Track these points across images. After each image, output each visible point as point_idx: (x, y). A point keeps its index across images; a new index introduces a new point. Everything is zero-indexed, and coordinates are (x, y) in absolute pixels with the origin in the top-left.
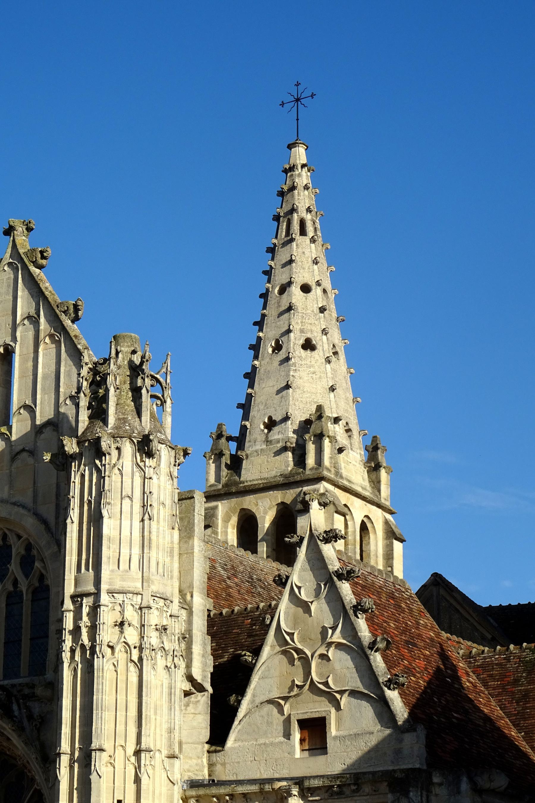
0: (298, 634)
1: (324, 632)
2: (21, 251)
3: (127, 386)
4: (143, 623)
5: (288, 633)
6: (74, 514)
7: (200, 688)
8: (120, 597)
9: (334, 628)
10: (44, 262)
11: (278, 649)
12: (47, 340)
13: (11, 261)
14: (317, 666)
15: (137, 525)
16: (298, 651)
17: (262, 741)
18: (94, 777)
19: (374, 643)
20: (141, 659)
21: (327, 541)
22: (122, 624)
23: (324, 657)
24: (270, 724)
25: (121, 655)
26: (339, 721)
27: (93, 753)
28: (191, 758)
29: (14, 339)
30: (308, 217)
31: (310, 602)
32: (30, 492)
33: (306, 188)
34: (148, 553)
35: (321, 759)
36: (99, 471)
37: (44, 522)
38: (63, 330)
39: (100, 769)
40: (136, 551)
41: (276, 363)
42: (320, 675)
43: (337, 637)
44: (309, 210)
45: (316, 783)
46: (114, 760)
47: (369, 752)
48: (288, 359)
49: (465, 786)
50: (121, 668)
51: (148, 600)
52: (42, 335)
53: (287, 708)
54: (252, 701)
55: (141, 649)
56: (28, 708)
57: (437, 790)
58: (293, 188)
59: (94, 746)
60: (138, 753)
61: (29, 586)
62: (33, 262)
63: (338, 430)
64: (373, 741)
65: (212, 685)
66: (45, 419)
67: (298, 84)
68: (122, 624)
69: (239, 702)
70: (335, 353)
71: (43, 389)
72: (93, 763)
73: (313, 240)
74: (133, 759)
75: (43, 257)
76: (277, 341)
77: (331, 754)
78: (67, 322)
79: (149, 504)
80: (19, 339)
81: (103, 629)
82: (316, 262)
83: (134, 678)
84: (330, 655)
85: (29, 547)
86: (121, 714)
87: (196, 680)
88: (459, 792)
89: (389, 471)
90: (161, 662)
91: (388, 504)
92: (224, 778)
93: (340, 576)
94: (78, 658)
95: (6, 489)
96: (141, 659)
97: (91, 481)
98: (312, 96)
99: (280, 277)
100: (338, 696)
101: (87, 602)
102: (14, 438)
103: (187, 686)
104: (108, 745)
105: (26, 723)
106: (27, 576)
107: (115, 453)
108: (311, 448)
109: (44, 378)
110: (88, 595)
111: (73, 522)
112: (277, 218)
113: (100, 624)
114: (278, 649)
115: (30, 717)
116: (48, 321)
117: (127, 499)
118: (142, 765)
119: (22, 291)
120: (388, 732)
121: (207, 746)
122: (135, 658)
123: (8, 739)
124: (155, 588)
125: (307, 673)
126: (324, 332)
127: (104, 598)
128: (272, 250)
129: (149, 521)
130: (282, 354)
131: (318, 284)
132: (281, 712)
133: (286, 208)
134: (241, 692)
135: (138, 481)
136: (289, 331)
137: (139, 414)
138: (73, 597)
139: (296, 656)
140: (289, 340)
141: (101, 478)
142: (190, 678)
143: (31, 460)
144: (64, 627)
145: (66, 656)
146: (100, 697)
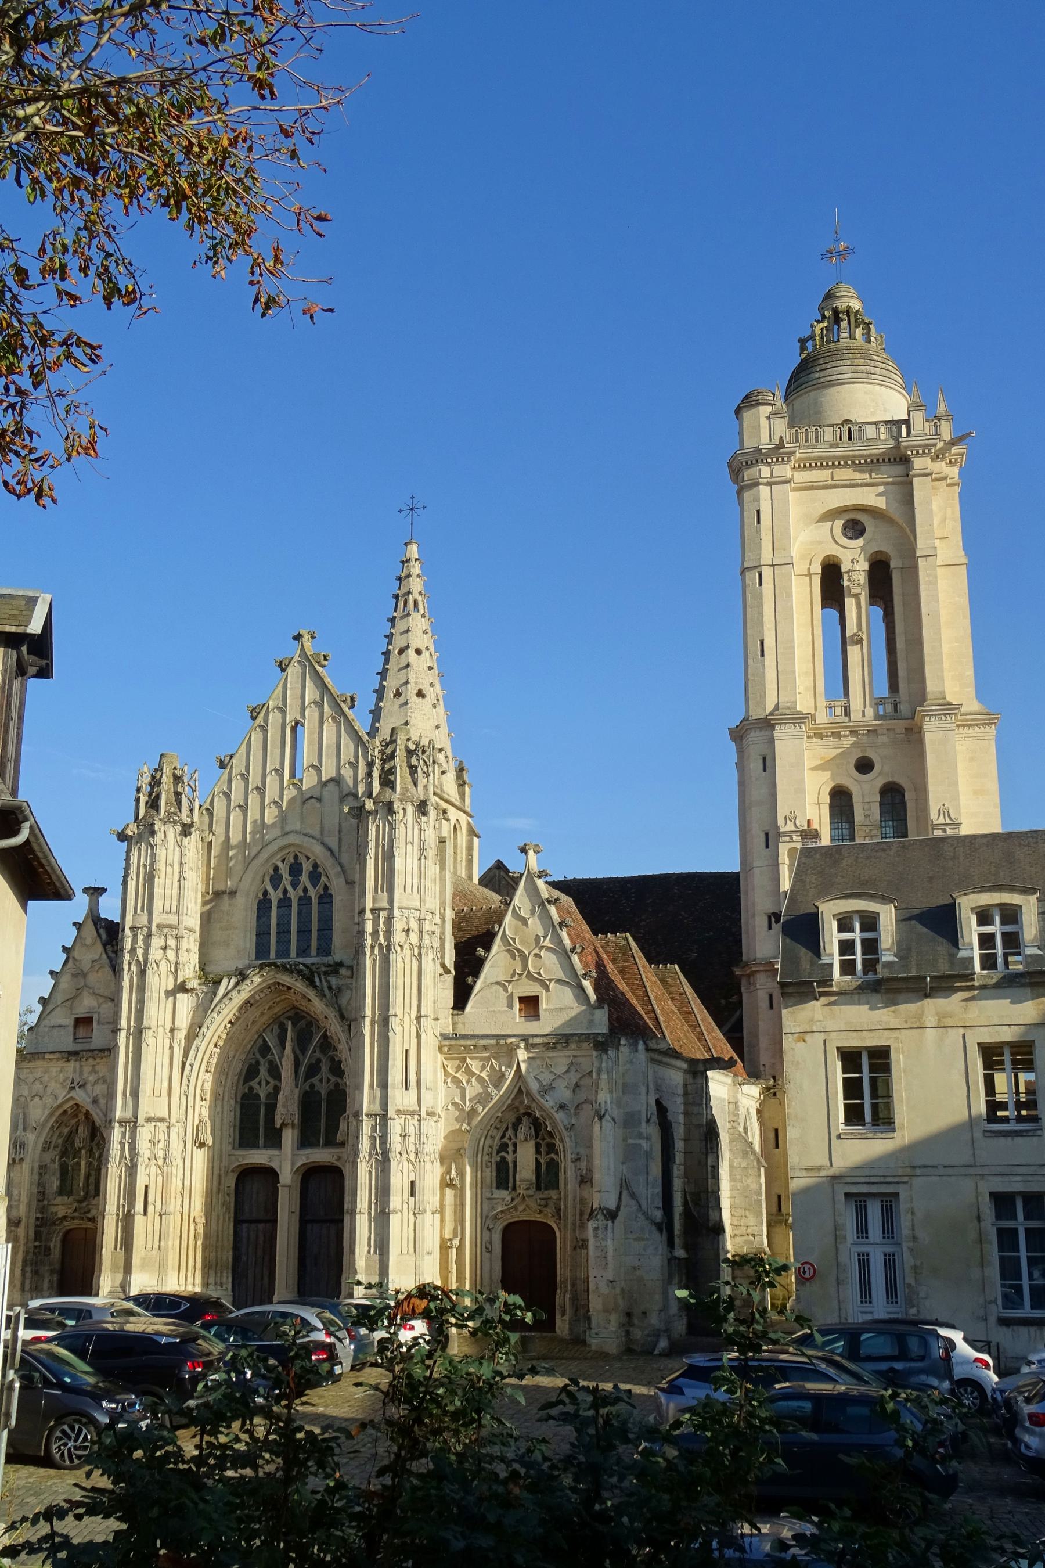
1: (537, 938)
2: (308, 654)
3: (405, 764)
6: (372, 852)
7: (447, 971)
8: (406, 912)
9: (545, 937)
10: (326, 663)
12: (330, 720)
15: (416, 862)
16: (518, 950)
17: (492, 1009)
19: (574, 948)
20: (420, 954)
21: (540, 877)
22: (408, 930)
24: (497, 998)
25: (407, 951)
29: (303, 716)
30: (420, 598)
32: (318, 828)
33: (418, 576)
35: (535, 1023)
36: (390, 823)
37: (330, 850)
38: (343, 713)
40: (416, 881)
41: (397, 706)
42: (534, 967)
43: (547, 943)
44: (420, 593)
45: (537, 1040)
47: (570, 1020)
48: (406, 703)
49: (641, 1046)
50: (407, 960)
52: (325, 717)
53: (510, 989)
54: (484, 982)
55: (420, 948)
56: (328, 981)
57: (622, 1049)
58: (409, 576)
59: (390, 1013)
60: (419, 1018)
61: (317, 892)
63: (440, 757)
64: (573, 1013)
65: (455, 969)
66: (328, 777)
67: (412, 498)
68: (408, 930)
69: (475, 982)
71: (327, 755)
73: (423, 616)
74: (415, 1022)
75: (325, 659)
76: (398, 690)
78: (346, 709)
82: (425, 632)
83: (415, 968)
85: (316, 866)
86: (407, 991)
88: (637, 1051)
89: (470, 787)
90: (431, 956)
91: (468, 809)
92: (464, 1033)
93: (550, 902)
94: (376, 951)
95: (299, 824)
96: (420, 954)
97: (384, 830)
98: (424, 507)
99: (399, 642)
101: (383, 915)
102: (304, 788)
103: (441, 970)
104: (399, 1013)
105: (326, 991)
106: (314, 886)
107: (401, 812)
109: (328, 746)
112: (396, 597)
114: (503, 948)
115: (330, 988)
116: (330, 706)
119: (309, 684)
120: (583, 1008)
122: (416, 953)
123: (309, 1000)
124: (427, 906)
125: (525, 965)
126: (432, 685)
127: (396, 913)
128: (392, 620)
130: (402, 700)
131: (427, 649)
132: (506, 990)
133: (404, 590)
134: (476, 974)
135: (417, 832)
136: (407, 683)
137: (415, 784)
138: (372, 910)
140: (407, 689)
141: (392, 829)
142: (443, 965)
143: (318, 805)
145: (368, 950)
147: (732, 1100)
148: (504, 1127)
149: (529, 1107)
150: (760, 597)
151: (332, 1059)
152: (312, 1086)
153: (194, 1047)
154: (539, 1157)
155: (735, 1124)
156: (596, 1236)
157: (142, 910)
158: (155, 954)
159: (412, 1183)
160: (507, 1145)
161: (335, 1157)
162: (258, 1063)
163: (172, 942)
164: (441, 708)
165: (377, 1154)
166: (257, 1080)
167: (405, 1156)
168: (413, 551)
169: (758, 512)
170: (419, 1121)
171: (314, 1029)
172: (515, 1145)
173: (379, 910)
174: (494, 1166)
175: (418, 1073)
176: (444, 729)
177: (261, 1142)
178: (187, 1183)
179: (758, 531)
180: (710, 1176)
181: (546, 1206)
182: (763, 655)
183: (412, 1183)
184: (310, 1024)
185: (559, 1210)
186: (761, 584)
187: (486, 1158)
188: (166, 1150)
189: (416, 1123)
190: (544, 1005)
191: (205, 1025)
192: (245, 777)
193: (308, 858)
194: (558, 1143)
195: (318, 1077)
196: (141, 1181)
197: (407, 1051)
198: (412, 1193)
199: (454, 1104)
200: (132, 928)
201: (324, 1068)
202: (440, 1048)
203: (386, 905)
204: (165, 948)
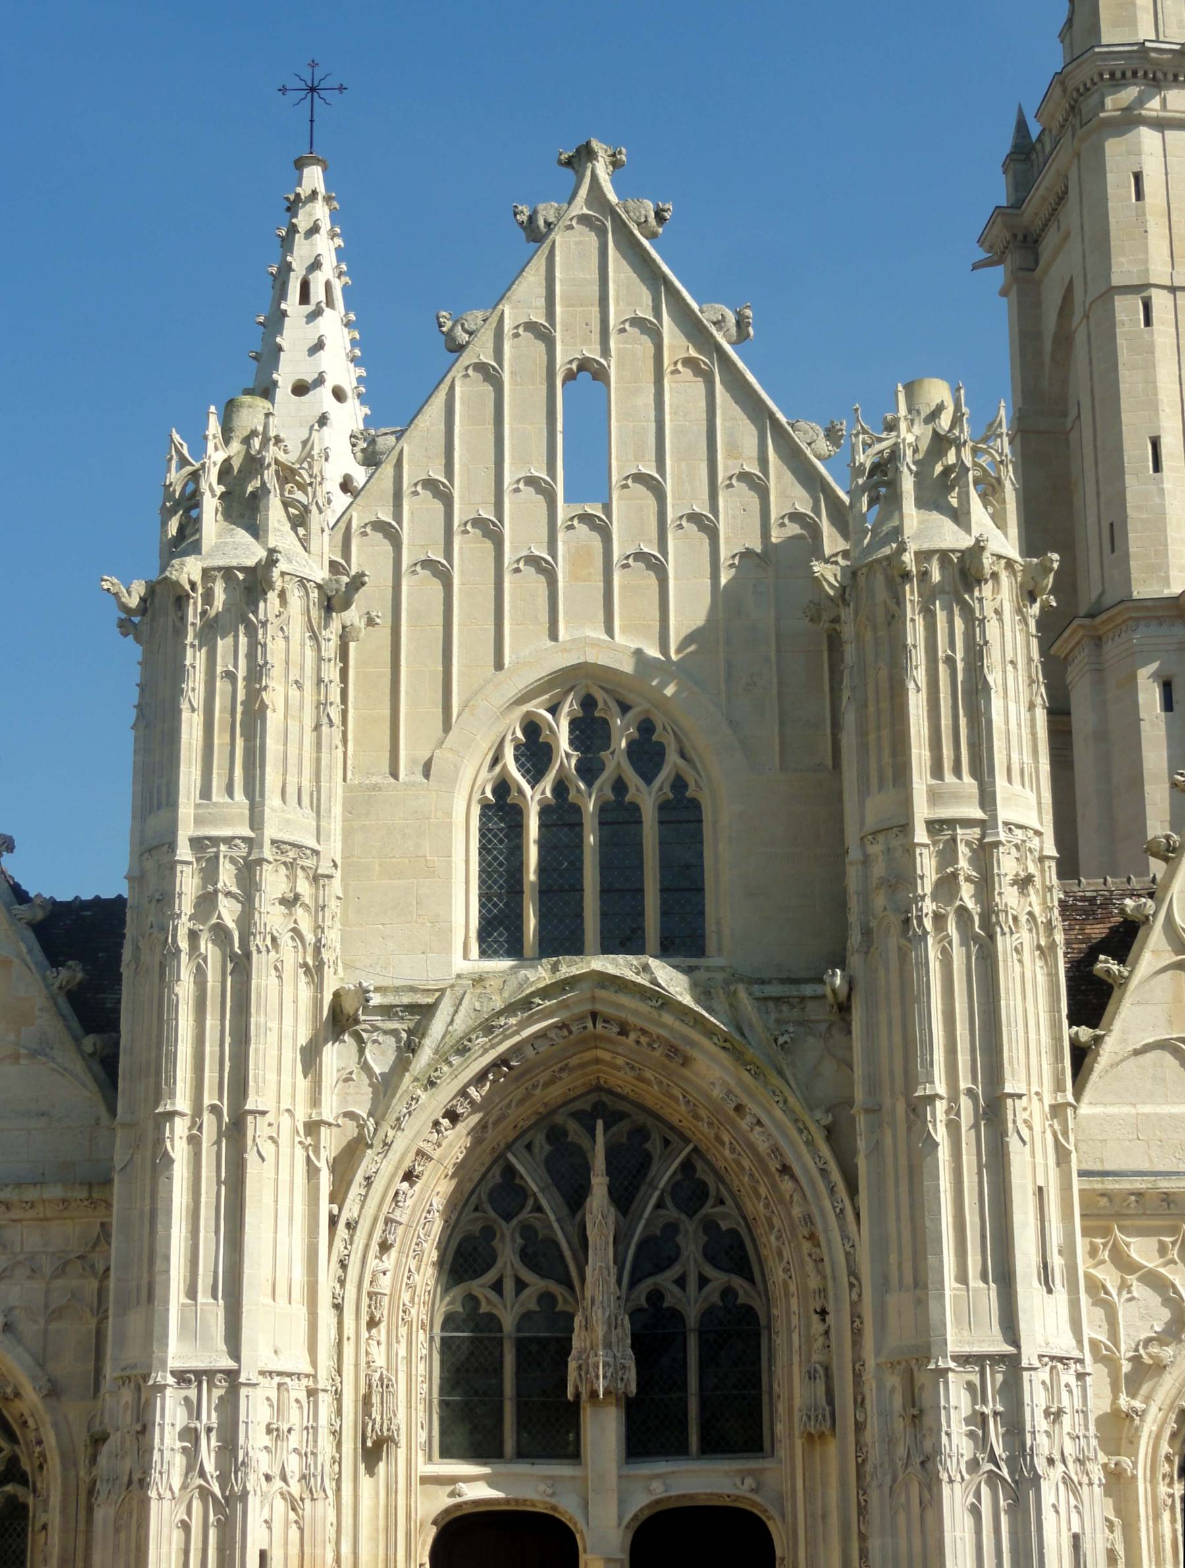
10: (660, 230)
13: (585, 211)
27: (1009, 1101)
62: (639, 224)
67: (313, 65)
69: (1098, 1040)
72: (1010, 1117)
80: (613, 353)
85: (646, 727)
109: (679, 432)
110: (967, 823)
144: (919, 872)
146: (1012, 1003)
150: (1151, 349)
151: (710, 1226)
152: (656, 1296)
153: (359, 1177)
157: (230, 791)
158: (271, 917)
159: (1076, 1538)
161: (749, 1482)
162: (489, 1232)
163: (304, 887)
165: (993, 1459)
166: (491, 1276)
167: (1060, 1467)
168: (314, 177)
169: (1138, 177)
170: (1081, 1376)
171: (654, 1146)
173: (951, 823)
177: (509, 1445)
178: (346, 1549)
179: (1141, 214)
182: (1157, 467)
184: (640, 1133)
186: (1148, 322)
188: (308, 1455)
189: (1072, 1380)
191: (391, 1118)
192: (441, 492)
193: (625, 708)
195: (675, 1271)
196: (256, 1538)
200: (197, 843)
201: (691, 1246)
203: (978, 814)
204: (290, 902)
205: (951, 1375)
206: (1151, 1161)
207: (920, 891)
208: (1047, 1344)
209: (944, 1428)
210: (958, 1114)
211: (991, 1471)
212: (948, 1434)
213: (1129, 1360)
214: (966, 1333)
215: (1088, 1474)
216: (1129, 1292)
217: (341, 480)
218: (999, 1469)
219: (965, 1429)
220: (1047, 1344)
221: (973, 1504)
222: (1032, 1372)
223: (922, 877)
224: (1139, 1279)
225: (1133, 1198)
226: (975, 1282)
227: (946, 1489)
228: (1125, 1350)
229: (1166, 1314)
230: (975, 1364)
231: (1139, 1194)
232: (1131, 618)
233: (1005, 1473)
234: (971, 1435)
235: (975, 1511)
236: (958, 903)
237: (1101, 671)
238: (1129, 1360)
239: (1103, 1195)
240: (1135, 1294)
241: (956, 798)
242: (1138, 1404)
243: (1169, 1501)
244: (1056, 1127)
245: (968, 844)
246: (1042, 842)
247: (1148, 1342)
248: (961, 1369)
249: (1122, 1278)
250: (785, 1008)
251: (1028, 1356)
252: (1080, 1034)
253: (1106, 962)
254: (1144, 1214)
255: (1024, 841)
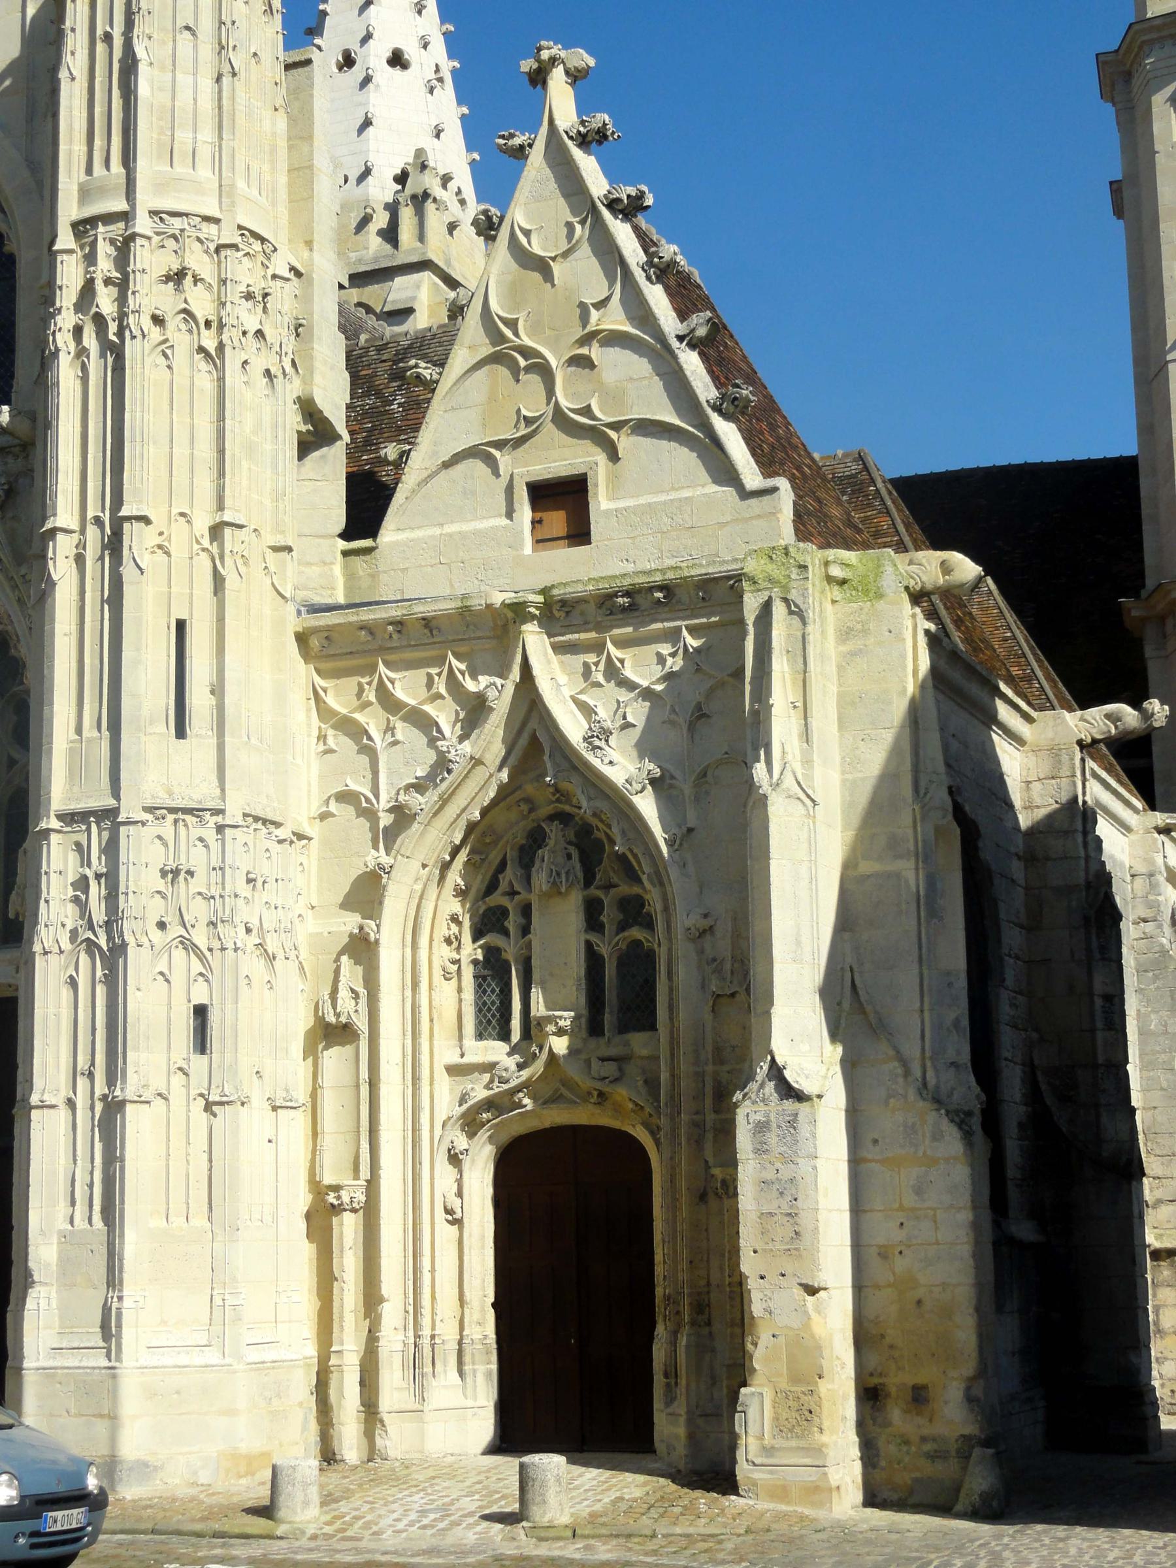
0: (526, 321)
4: (223, 276)
5: (506, 322)
11: (487, 350)
14: (566, 381)
15: (206, 83)
16: (526, 352)
18: (128, 571)
20: (221, 347)
23: (582, 362)
26: (615, 482)
27: (126, 526)
28: (309, 564)
31: (551, 258)
34: (230, 140)
39: (141, 556)
40: (206, 134)
46: (170, 541)
48: (367, 80)
51: (229, 235)
60: (216, 532)
63: (446, 196)
69: (404, 456)
70: (440, 80)
77: (599, 544)
79: (231, 45)
81: (142, 281)
84: (593, 356)
86: (181, 451)
87: (321, 412)
96: (221, 347)
100: (613, 435)
108: (407, 215)
110: (109, 218)
111: (73, 79)
113: (134, 272)
117: (187, 34)
118: (227, 552)
121: (342, 544)
125: (550, 392)
127: (143, 224)
129: (231, 78)
130: (357, 73)
139: (522, 363)
145: (63, 340)
146: (138, 415)
147: (1141, 868)
148: (495, 857)
149: (560, 794)
154: (593, 938)
155: (1149, 927)
156: (760, 1150)
159: (201, 1012)
160: (504, 912)
164: (447, 93)
165: (91, 928)
167: (175, 930)
170: (220, 829)
172: (526, 910)
173: (92, 221)
174: (468, 973)
175: (218, 690)
176: (455, 134)
180: (1099, 1025)
181: (616, 1080)
183: (201, 1012)
185: (652, 1085)
187: (447, 952)
189: (210, 835)
190: (601, 502)
194: (653, 897)
197: (181, 625)
198: (201, 1042)
199: (346, 797)
202: (302, 638)
203: (119, 205)
205: (54, 838)
206: (452, 586)
207: (58, 304)
208: (170, 794)
209: (44, 895)
210: (84, 548)
211: (88, 939)
212: (47, 901)
213: (390, 810)
214: (76, 789)
215: (220, 939)
216: (393, 735)
217: (389, 54)
218: (96, 937)
219: (71, 892)
220: (170, 794)
221: (71, 977)
222: (131, 828)
223: (60, 288)
224: (404, 719)
225: (390, 628)
226: (89, 731)
227: (39, 962)
228: (384, 802)
229: (431, 757)
230: (82, 822)
231: (399, 624)
232: (1143, 42)
233: (102, 941)
234: (76, 900)
235: (73, 983)
236: (94, 310)
237: (1133, 108)
238: (390, 810)
239: (362, 628)
240: (399, 736)
241: (103, 191)
242: (386, 860)
243: (456, 967)
244: (215, 549)
245: (112, 242)
246: (219, 231)
247: (408, 787)
248: (69, 829)
249: (388, 719)
250: (10, 460)
251: (129, 809)
252: (389, 454)
253: (416, 366)
254: (411, 646)
255: (182, 230)
